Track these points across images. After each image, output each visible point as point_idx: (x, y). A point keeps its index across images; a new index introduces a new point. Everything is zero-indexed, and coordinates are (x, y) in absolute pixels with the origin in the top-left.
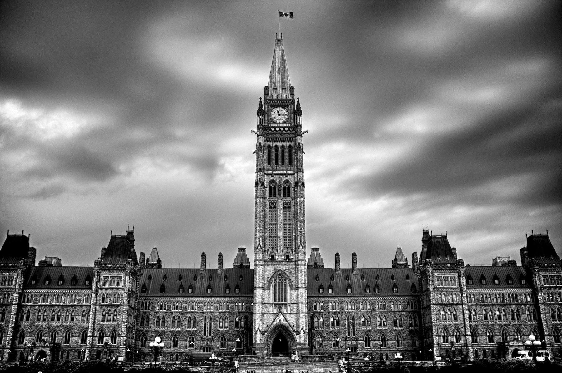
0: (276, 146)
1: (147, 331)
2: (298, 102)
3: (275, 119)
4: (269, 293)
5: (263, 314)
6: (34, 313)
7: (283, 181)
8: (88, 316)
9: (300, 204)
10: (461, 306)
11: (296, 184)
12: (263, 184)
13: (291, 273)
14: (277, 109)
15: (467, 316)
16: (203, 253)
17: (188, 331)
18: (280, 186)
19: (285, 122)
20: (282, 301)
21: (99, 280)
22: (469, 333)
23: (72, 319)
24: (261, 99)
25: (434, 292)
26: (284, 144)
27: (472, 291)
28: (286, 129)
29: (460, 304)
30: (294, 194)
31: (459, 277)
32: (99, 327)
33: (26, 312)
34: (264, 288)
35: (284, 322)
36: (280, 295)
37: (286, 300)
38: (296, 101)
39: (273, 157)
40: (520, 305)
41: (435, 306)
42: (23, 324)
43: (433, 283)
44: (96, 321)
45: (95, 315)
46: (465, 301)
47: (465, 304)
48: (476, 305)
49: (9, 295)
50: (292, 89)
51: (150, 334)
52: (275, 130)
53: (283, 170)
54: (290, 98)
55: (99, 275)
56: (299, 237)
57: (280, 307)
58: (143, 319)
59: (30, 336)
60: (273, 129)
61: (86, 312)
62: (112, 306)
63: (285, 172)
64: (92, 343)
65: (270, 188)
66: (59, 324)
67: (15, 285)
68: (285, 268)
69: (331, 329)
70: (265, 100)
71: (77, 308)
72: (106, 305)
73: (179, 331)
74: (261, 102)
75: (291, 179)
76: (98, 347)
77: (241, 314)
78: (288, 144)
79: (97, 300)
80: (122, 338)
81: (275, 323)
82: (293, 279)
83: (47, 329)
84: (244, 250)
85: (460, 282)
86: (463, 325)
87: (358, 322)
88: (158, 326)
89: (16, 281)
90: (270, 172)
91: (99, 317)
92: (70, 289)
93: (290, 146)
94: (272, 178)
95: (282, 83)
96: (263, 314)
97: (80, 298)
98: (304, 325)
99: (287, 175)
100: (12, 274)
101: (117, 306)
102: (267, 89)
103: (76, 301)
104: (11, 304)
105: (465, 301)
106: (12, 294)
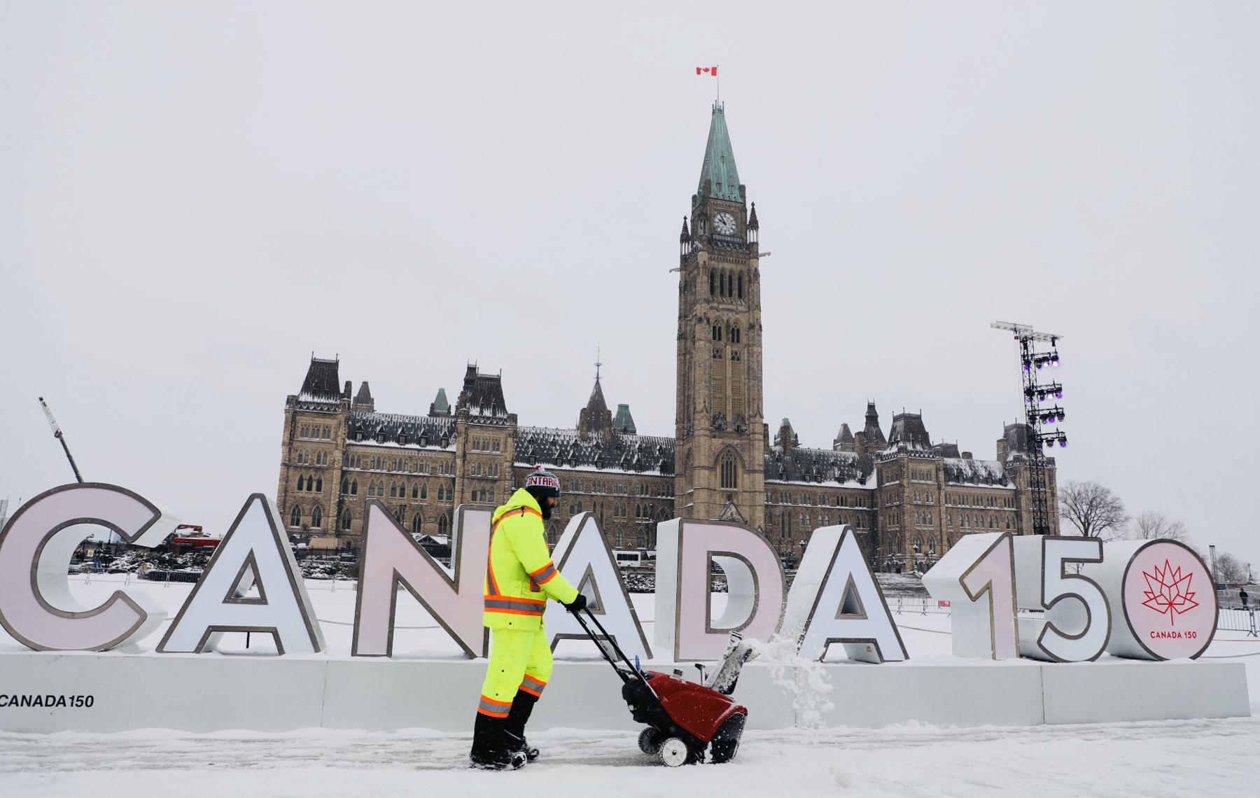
0: (723, 269)
2: (753, 210)
6: (364, 485)
8: (450, 492)
11: (752, 327)
12: (708, 320)
19: (731, 236)
23: (424, 496)
26: (734, 266)
27: (949, 489)
31: (938, 470)
36: (729, 478)
38: (749, 208)
39: (717, 284)
45: (462, 492)
46: (943, 500)
49: (325, 455)
50: (742, 188)
62: (488, 480)
63: (733, 307)
67: (335, 439)
72: (478, 479)
75: (744, 320)
82: (746, 458)
84: (626, 407)
85: (937, 477)
89: (336, 433)
100: (328, 421)
101: (496, 481)
104: (331, 468)
105: (943, 500)
106: (331, 453)
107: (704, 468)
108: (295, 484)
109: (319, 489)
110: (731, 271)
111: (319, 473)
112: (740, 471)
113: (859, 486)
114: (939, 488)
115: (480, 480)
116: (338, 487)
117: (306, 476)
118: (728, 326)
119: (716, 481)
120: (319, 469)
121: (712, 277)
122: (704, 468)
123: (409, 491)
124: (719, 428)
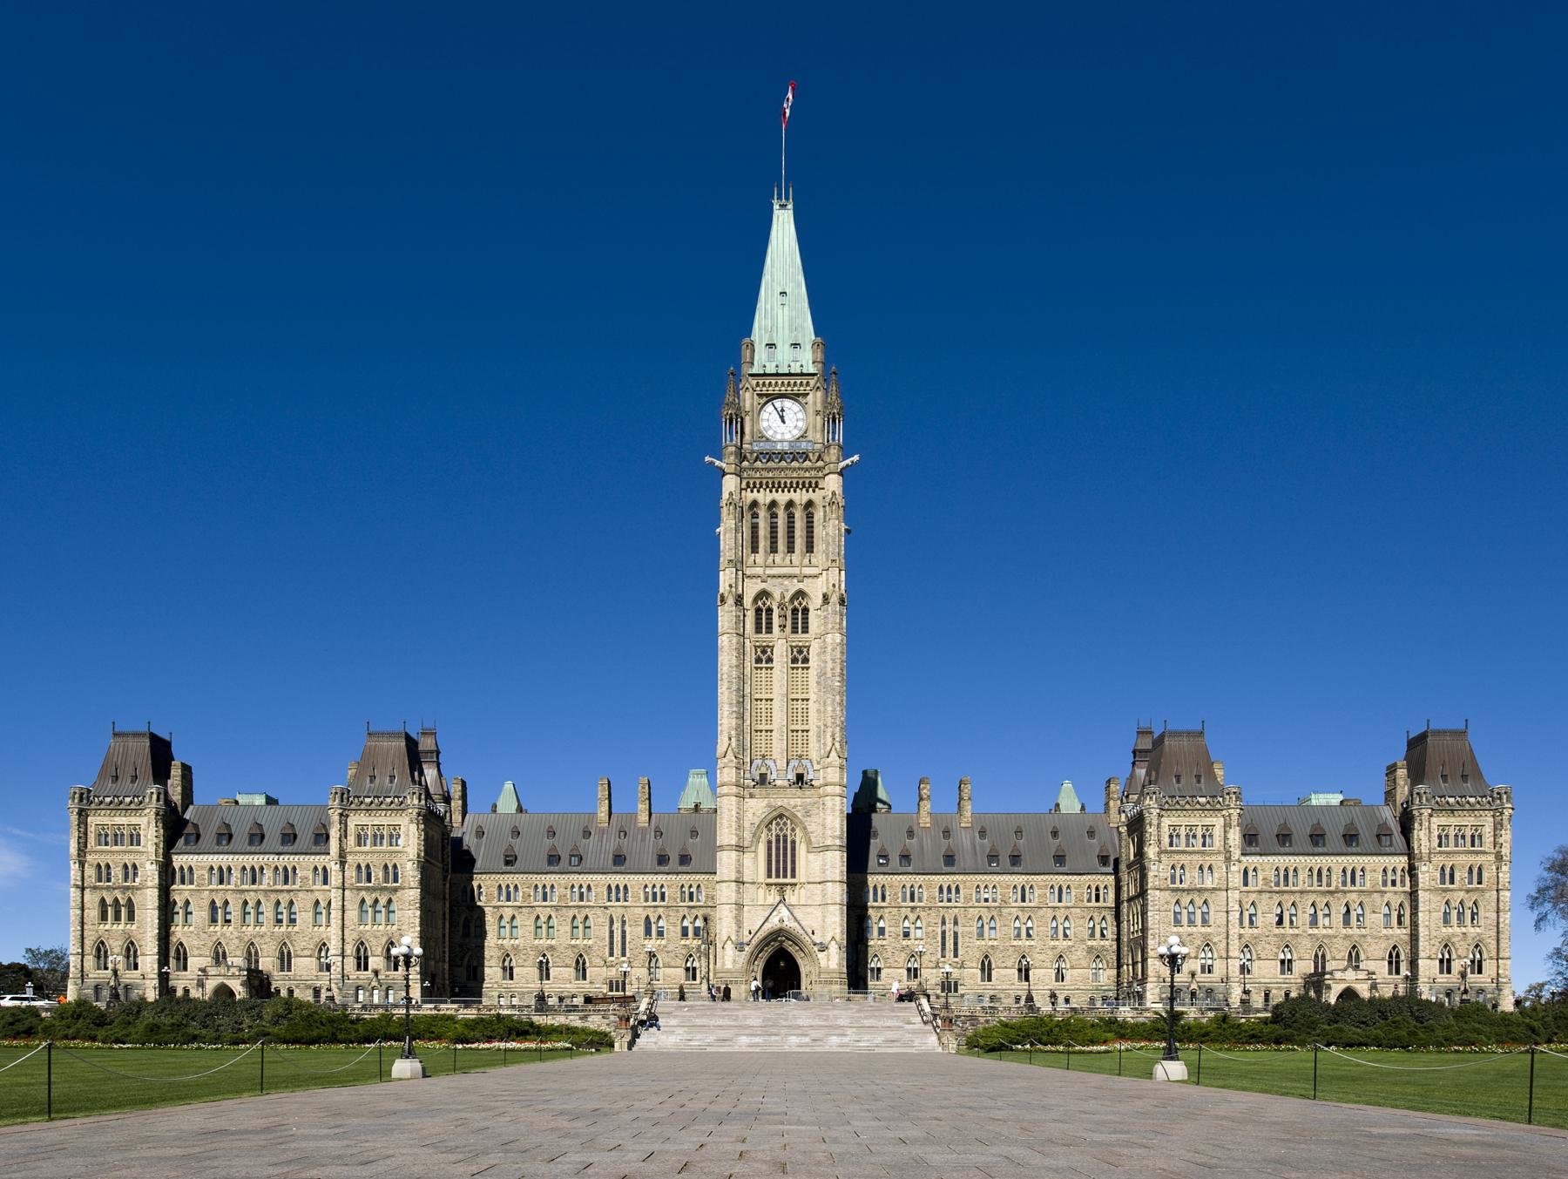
4: (756, 858)
5: (740, 906)
13: (807, 814)
14: (778, 403)
15: (1235, 916)
20: (785, 876)
33: (180, 904)
34: (740, 848)
35: (790, 924)
36: (782, 861)
37: (793, 876)
40: (1371, 893)
42: (179, 932)
48: (1260, 892)
54: (812, 371)
57: (782, 892)
61: (323, 904)
62: (386, 888)
68: (793, 801)
71: (301, 894)
72: (367, 889)
77: (695, 911)
81: (768, 927)
82: (810, 829)
91: (352, 914)
92: (279, 854)
95: (791, 331)
96: (740, 906)
103: (298, 880)
107: (730, 847)
108: (93, 913)
109: (131, 917)
111: (129, 893)
112: (801, 850)
115: (374, 889)
116: (156, 913)
117: (109, 901)
119: (755, 865)
120: (128, 888)
122: (730, 847)
124: (763, 780)
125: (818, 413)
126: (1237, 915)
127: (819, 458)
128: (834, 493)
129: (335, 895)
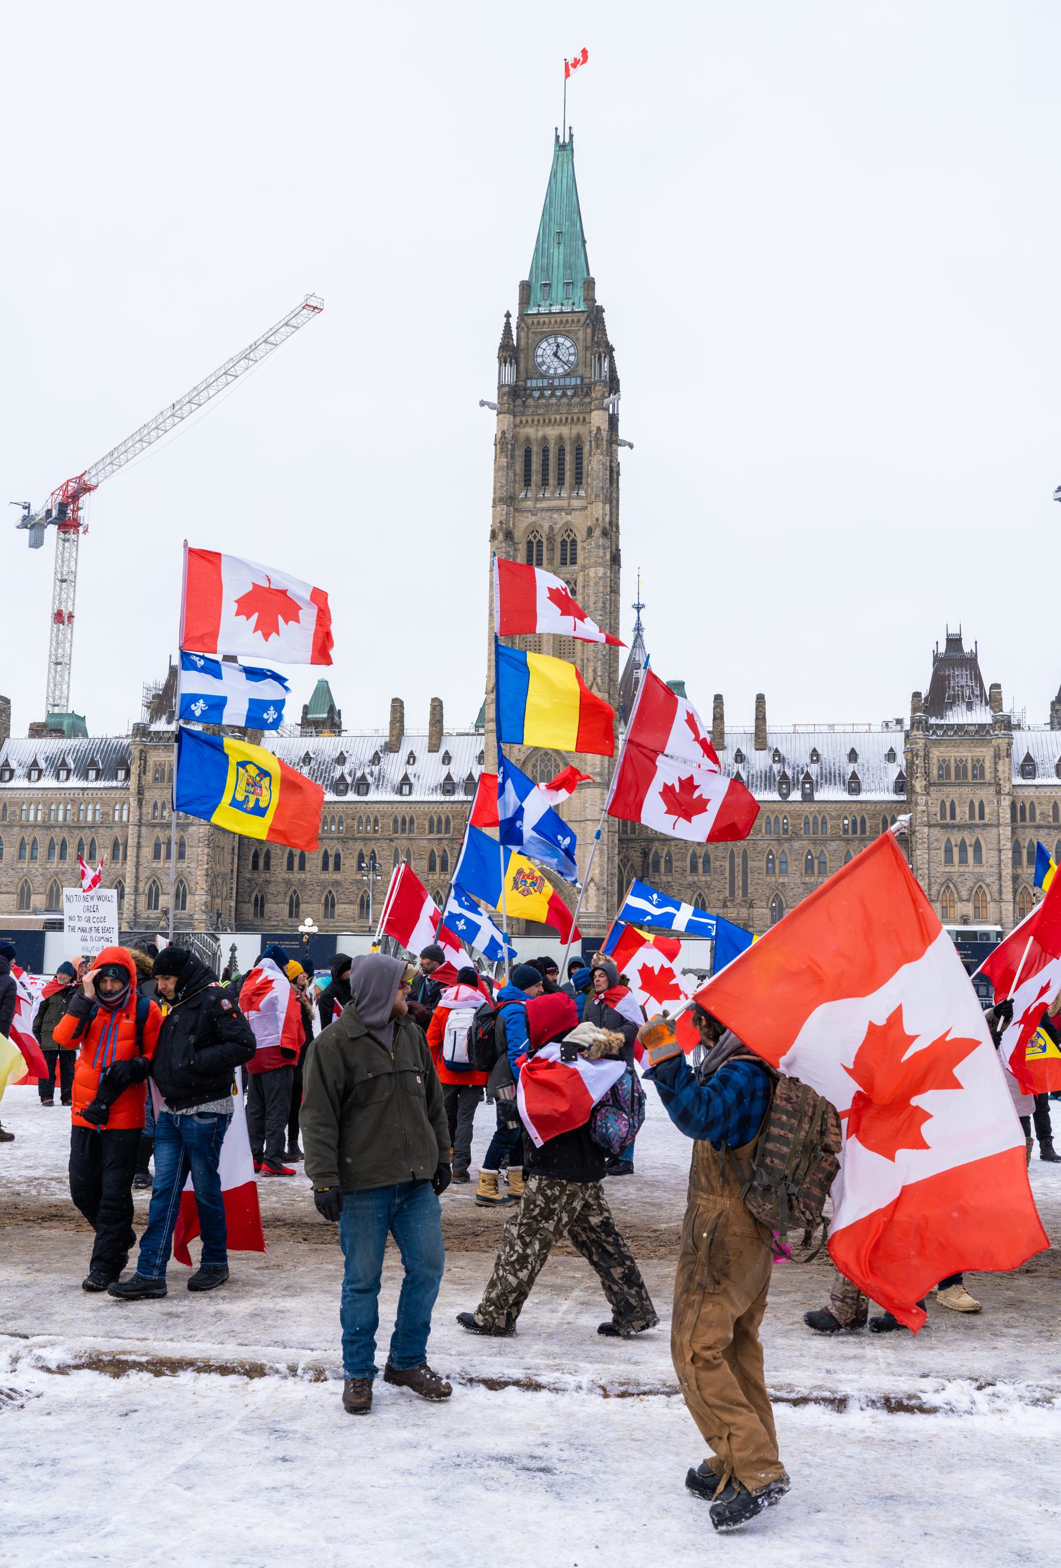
0: (545, 438)
1: (268, 882)
3: (544, 368)
7: (558, 526)
9: (596, 584)
10: (995, 830)
11: (590, 531)
12: (509, 535)
14: (551, 340)
15: (1007, 855)
16: (395, 701)
17: (357, 881)
18: (551, 539)
19: (567, 375)
21: (143, 770)
22: (1008, 895)
24: (508, 315)
25: (928, 794)
26: (565, 431)
28: (569, 393)
29: (991, 825)
30: (585, 559)
32: (147, 873)
41: (926, 829)
43: (927, 774)
44: (142, 860)
45: (139, 846)
47: (1006, 825)
50: (590, 284)
51: (272, 889)
52: (542, 396)
53: (560, 498)
55: (143, 757)
56: (592, 664)
58: (256, 856)
59: (8, 893)
60: (536, 394)
63: (564, 503)
64: (135, 908)
65: (530, 544)
66: (66, 866)
69: (690, 879)
70: (522, 316)
71: (101, 830)
73: (337, 883)
74: (508, 325)
75: (579, 522)
76: (148, 918)
78: (574, 432)
79: (141, 815)
80: (197, 897)
83: (40, 878)
86: (996, 877)
87: (756, 864)
88: (290, 867)
90: (529, 504)
91: (147, 852)
93: (579, 437)
94: (534, 518)
97: (106, 809)
98: (597, 871)
99: (569, 511)
102: (526, 288)
105: (1006, 815)
110: (560, 438)
113: (845, 796)
114: (998, 793)
118: (551, 539)
121: (528, 453)
123: (72, 850)
125: (586, 348)
126: (1010, 854)
127: (587, 394)
128: (599, 429)
129: (132, 831)
